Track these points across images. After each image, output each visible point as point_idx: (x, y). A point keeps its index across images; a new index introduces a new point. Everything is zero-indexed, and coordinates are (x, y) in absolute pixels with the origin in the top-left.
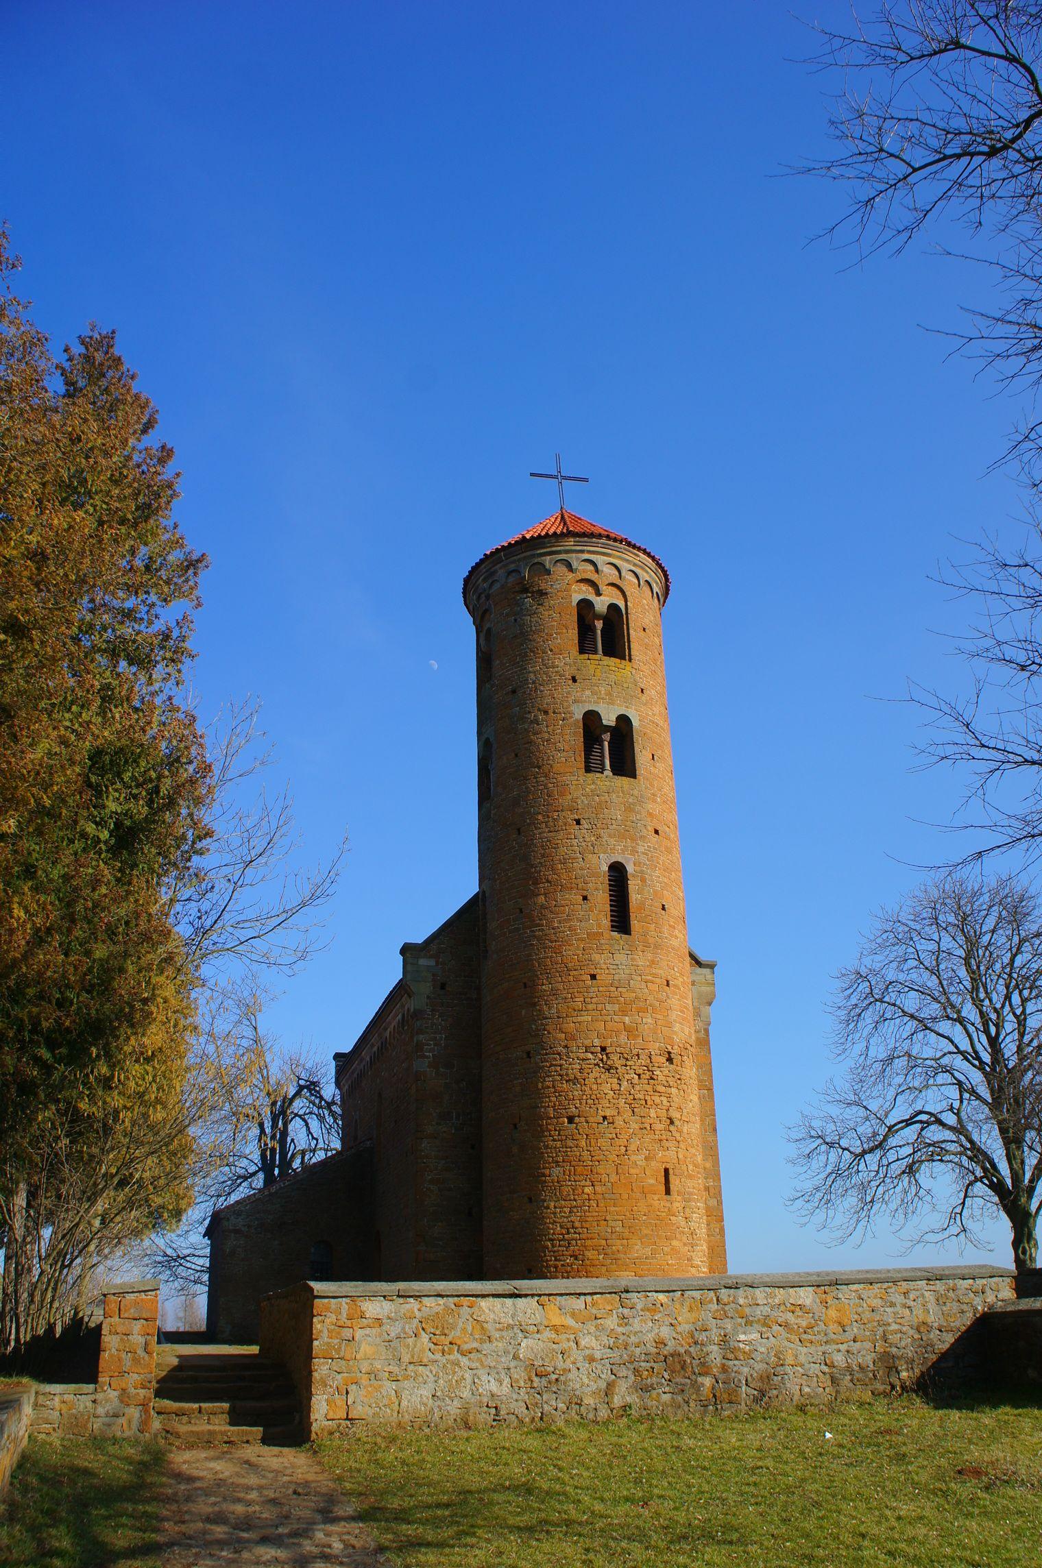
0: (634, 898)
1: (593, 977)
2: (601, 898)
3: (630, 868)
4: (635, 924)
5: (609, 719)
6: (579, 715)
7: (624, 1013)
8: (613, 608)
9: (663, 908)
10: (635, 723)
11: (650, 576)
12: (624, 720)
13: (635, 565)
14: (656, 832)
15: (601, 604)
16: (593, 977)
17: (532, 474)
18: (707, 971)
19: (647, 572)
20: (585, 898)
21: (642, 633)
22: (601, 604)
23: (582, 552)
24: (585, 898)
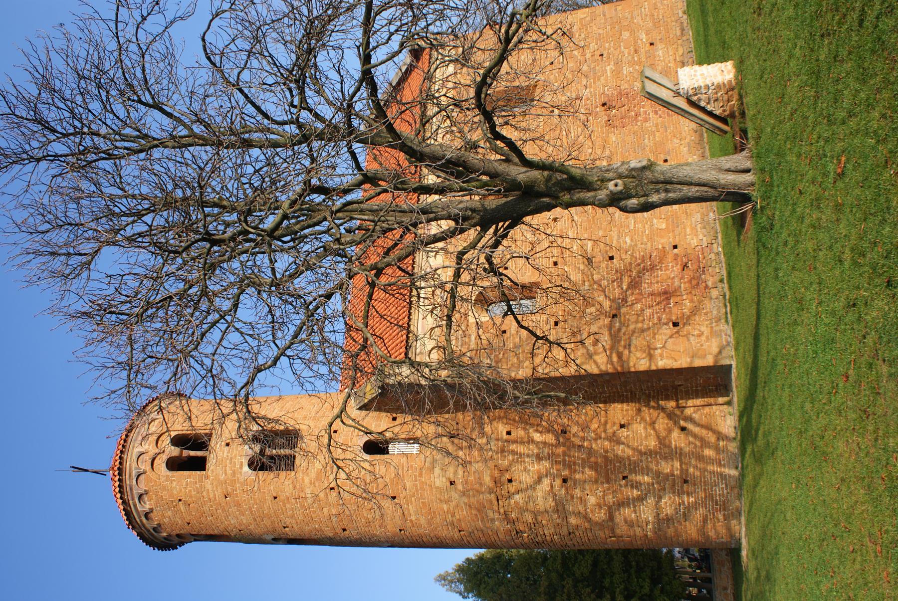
11: (140, 517)
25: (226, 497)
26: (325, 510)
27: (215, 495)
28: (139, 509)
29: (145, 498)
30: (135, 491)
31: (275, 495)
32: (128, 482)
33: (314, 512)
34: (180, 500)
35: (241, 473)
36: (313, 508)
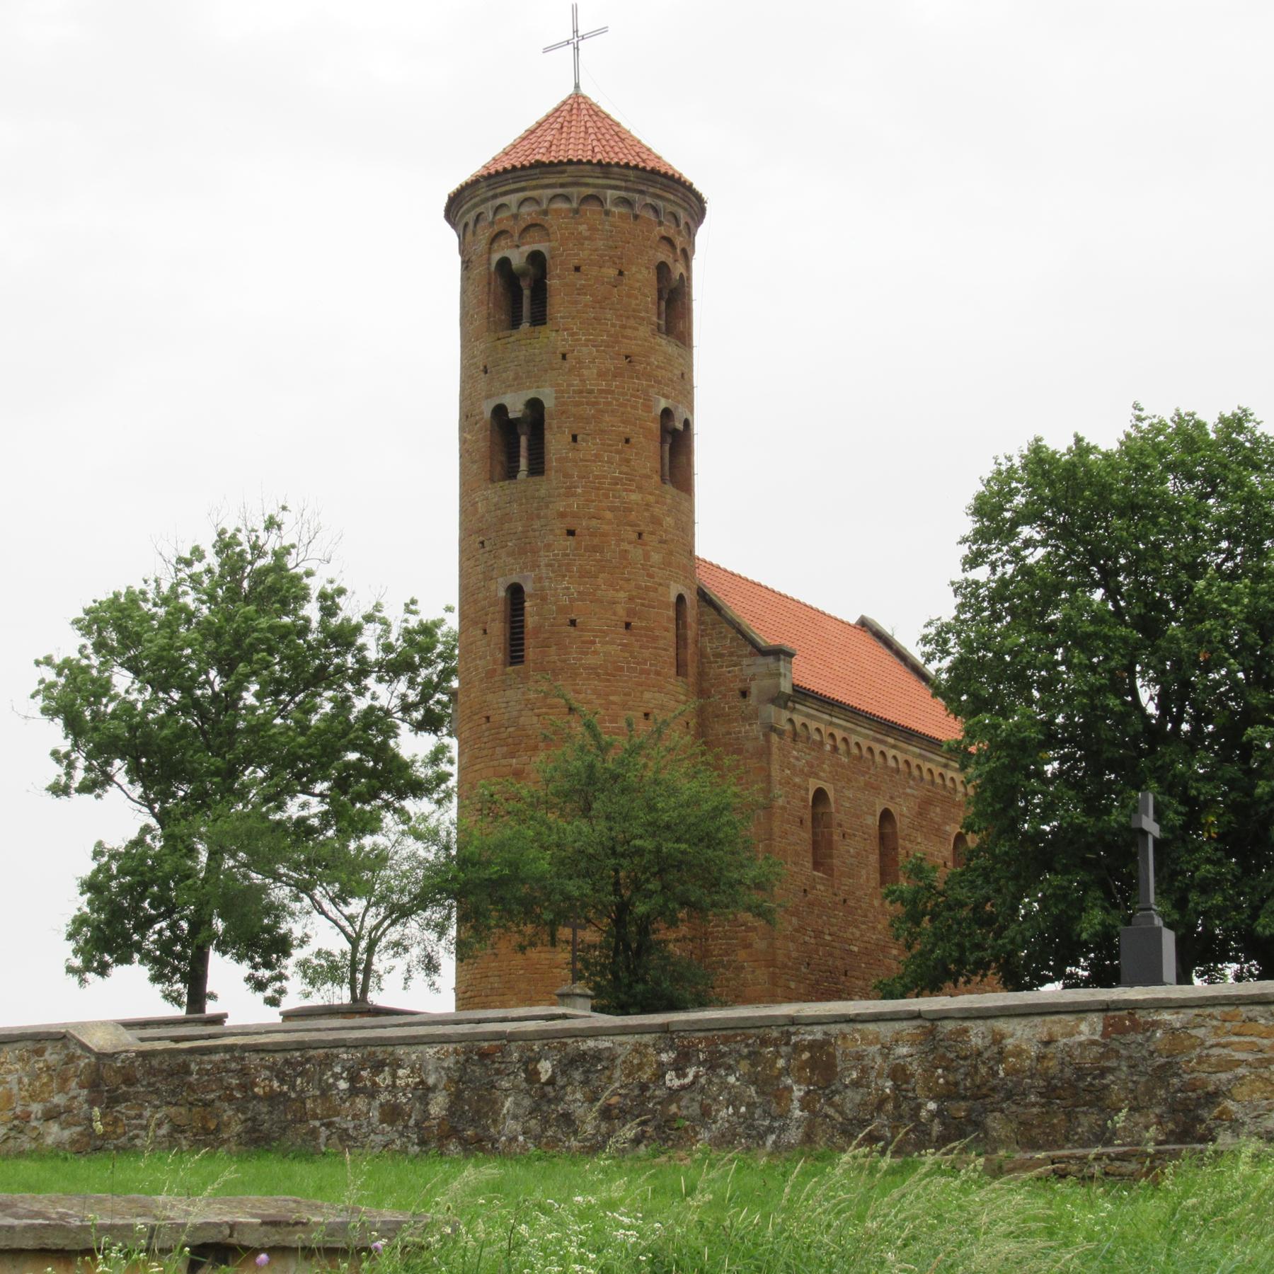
0: (530, 621)
1: (488, 718)
2: (498, 628)
3: (528, 588)
4: (530, 653)
5: (516, 406)
6: (487, 414)
7: (512, 755)
8: (537, 259)
9: (573, 623)
10: (549, 403)
11: (595, 186)
12: (535, 406)
13: (562, 185)
14: (571, 533)
15: (518, 258)
16: (488, 718)
17: (546, 50)
18: (770, 659)
19: (587, 185)
20: (485, 632)
21: (572, 277)
22: (518, 258)
23: (495, 197)
24: (485, 632)
25: (627, 357)
26: (609, 515)
27: (630, 339)
28: (609, 192)
29: (623, 210)
30: (637, 196)
31: (632, 441)
32: (652, 190)
33: (607, 496)
34: (621, 273)
35: (658, 394)
36: (614, 496)
